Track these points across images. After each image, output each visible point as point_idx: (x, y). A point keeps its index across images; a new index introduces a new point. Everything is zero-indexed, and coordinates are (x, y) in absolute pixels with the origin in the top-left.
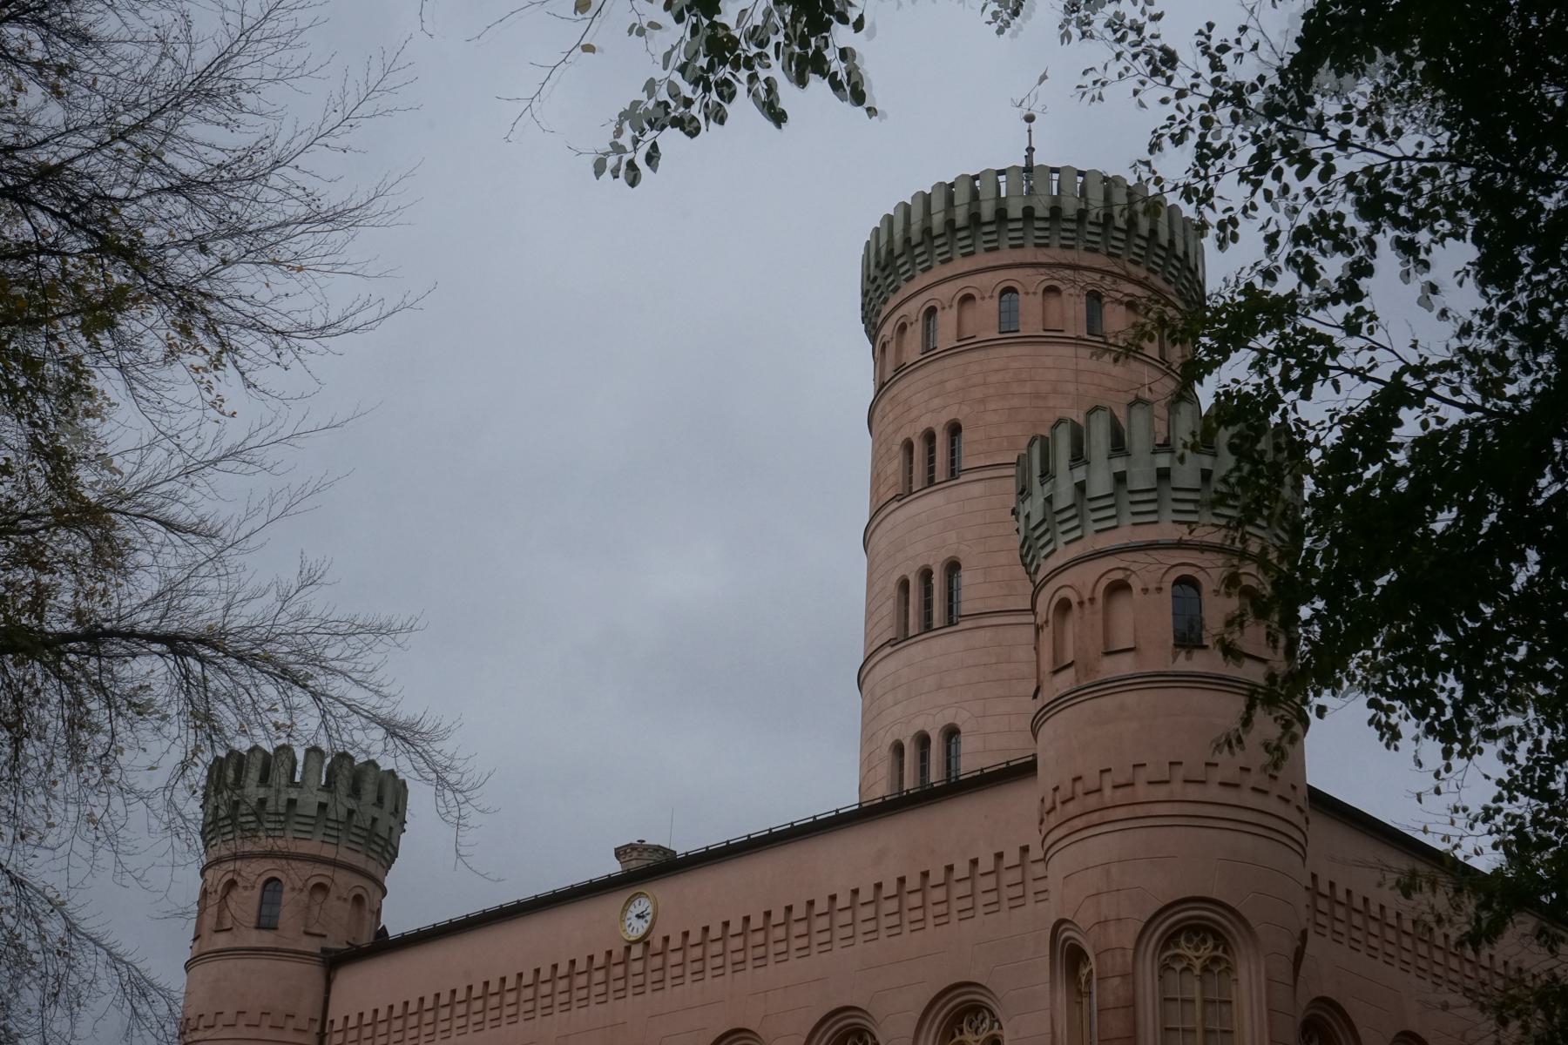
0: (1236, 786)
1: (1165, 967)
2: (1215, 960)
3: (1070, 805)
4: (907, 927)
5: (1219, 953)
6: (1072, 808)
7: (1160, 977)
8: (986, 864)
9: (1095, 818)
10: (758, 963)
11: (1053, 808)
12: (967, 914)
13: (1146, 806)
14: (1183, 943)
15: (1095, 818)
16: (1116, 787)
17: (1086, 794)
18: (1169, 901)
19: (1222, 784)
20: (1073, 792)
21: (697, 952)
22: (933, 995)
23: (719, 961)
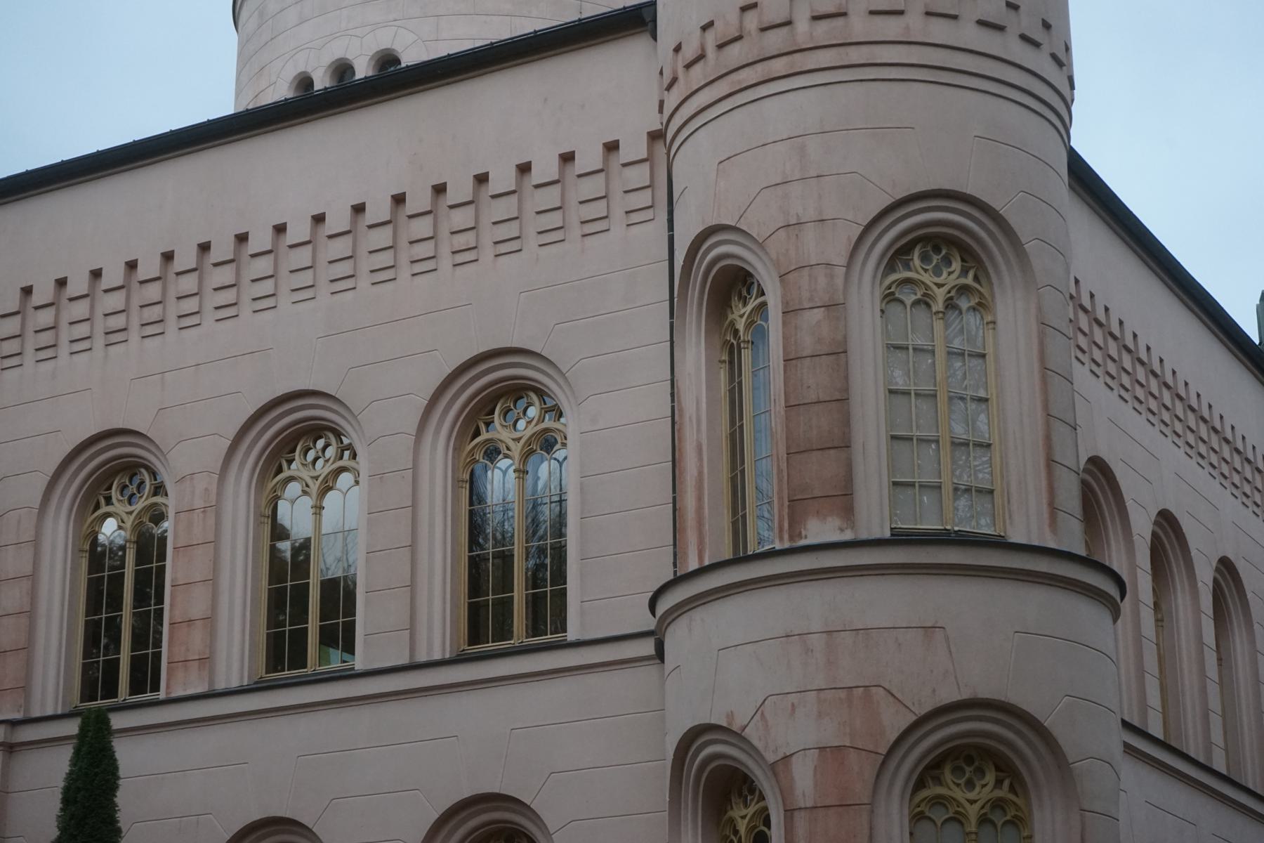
0: (1000, 28)
1: (890, 298)
2: (964, 290)
3: (734, 50)
4: (405, 271)
5: (969, 280)
6: (736, 53)
7: (882, 311)
8: (546, 168)
9: (779, 66)
10: (150, 330)
11: (701, 57)
12: (509, 246)
13: (864, 48)
14: (917, 261)
15: (779, 66)
16: (816, 18)
17: (763, 30)
18: (900, 194)
19: (981, 23)
20: (741, 27)
21: (46, 317)
22: (448, 370)
23: (82, 330)
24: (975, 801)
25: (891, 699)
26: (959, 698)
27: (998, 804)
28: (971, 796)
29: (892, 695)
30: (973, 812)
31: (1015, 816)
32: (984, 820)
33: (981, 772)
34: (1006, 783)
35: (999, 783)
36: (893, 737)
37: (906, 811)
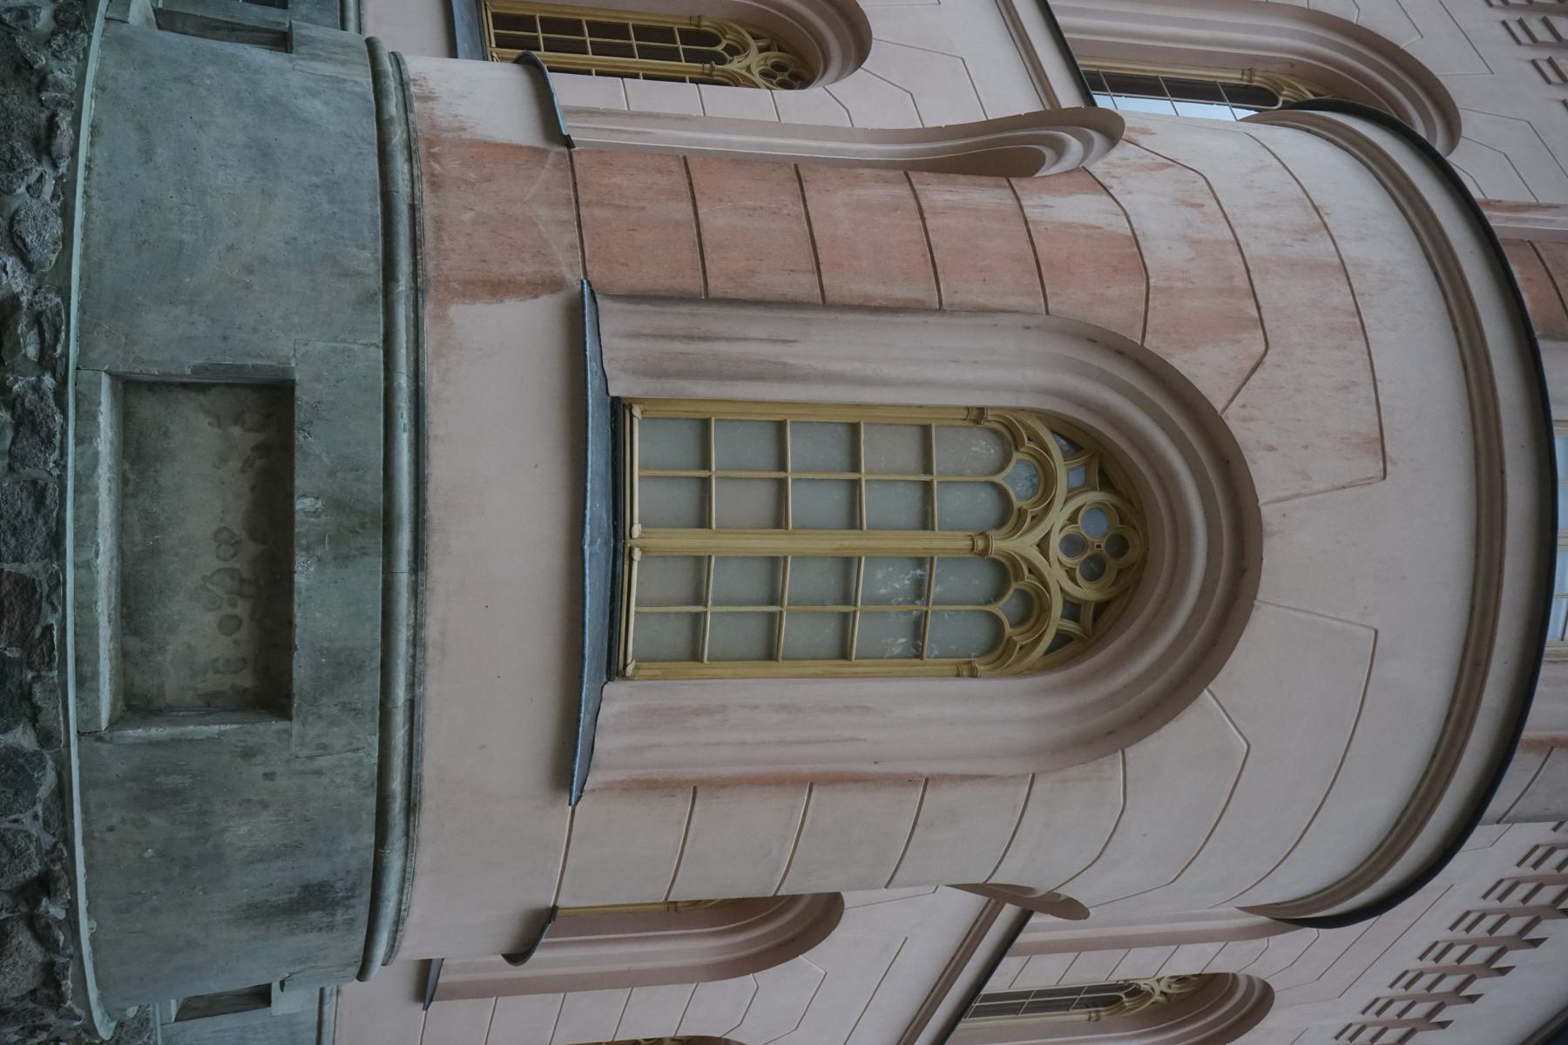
24: (1045, 554)
25: (1249, 365)
26: (1261, 501)
27: (1033, 607)
28: (1055, 541)
29: (1253, 370)
30: (1023, 545)
31: (1010, 644)
32: (1005, 571)
33: (1094, 571)
34: (1069, 626)
35: (1073, 609)
36: (1181, 362)
37: (1026, 401)
